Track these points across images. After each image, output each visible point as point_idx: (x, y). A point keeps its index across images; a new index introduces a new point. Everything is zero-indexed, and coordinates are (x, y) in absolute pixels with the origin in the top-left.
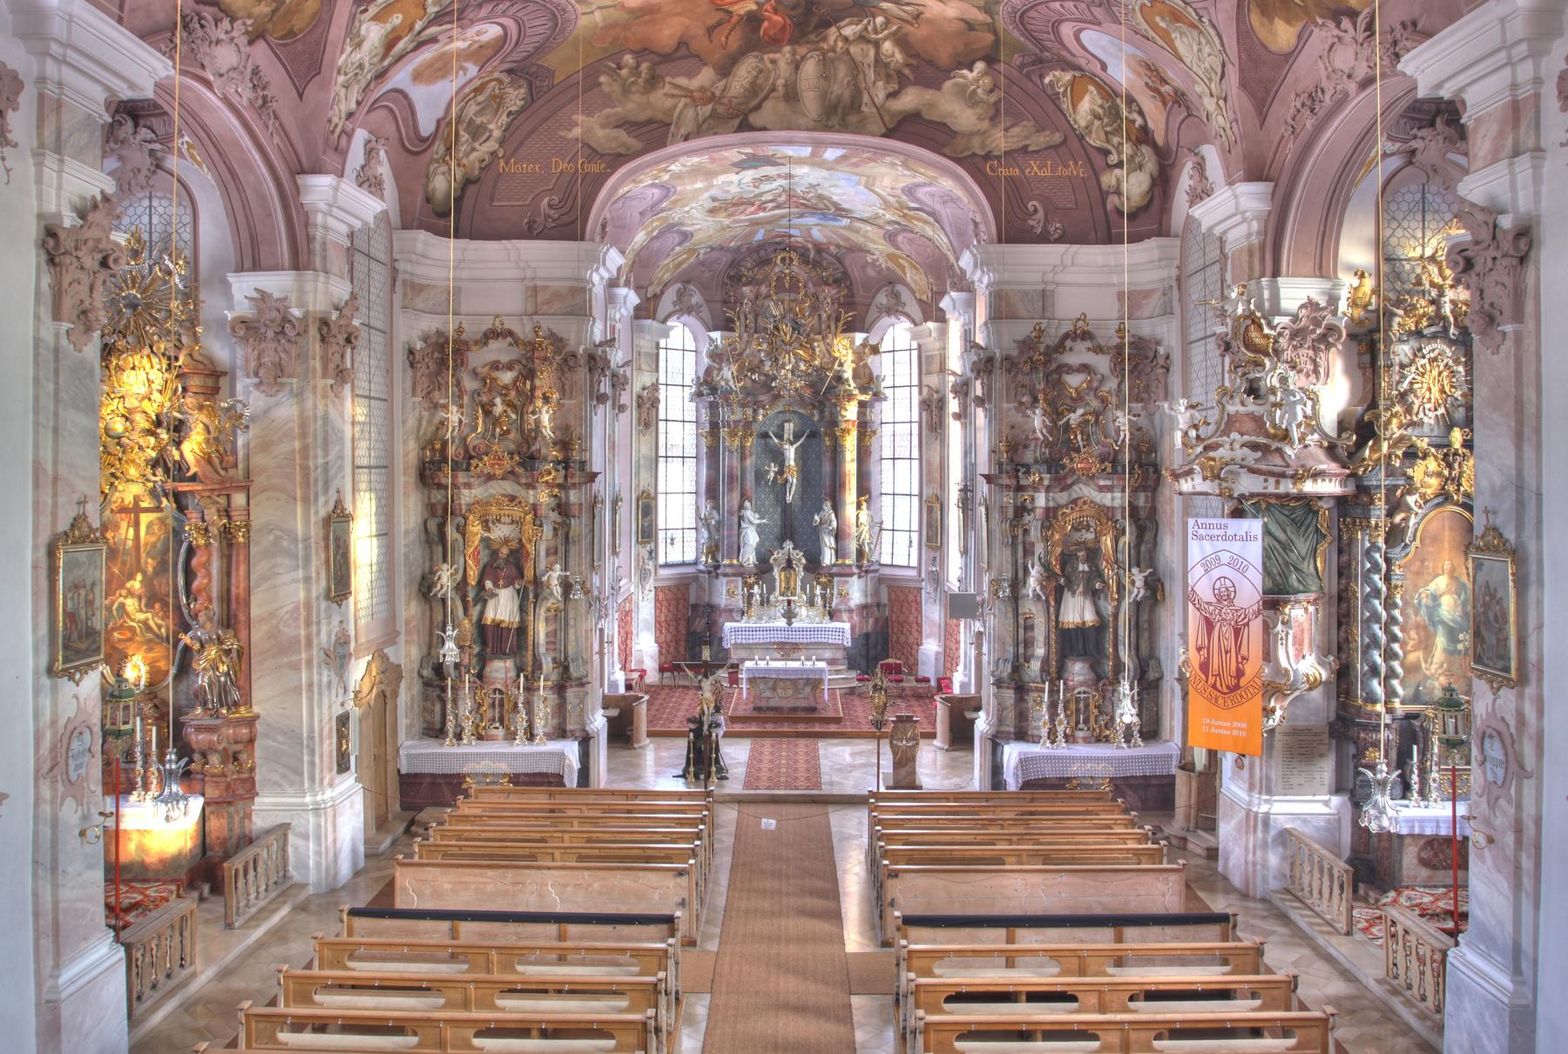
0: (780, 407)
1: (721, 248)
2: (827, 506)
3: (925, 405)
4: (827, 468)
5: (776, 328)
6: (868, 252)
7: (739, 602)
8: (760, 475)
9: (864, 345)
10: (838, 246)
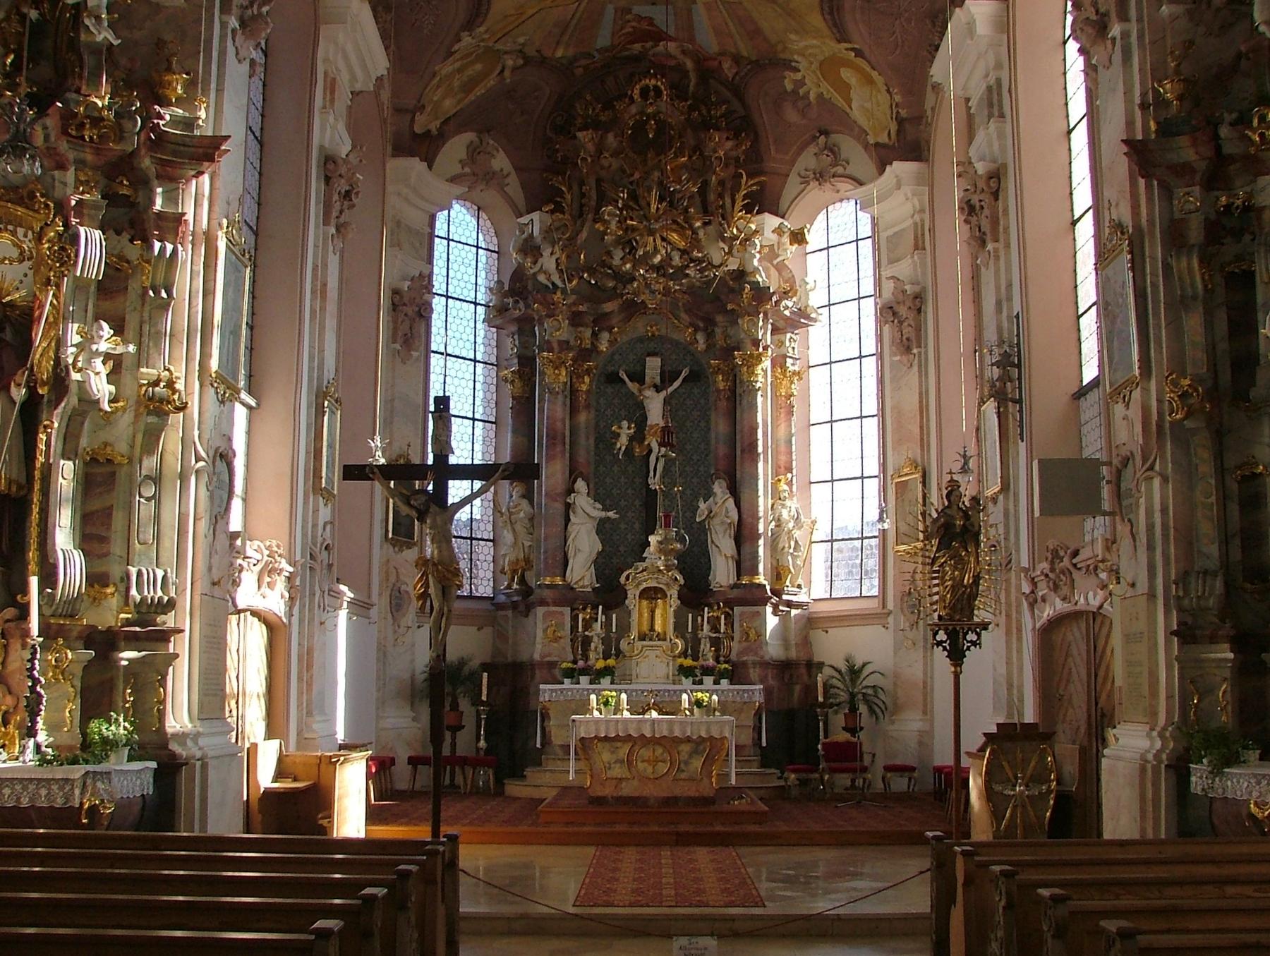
0: (640, 326)
1: (542, 62)
2: (719, 488)
3: (888, 313)
4: (720, 426)
5: (633, 196)
6: (789, 66)
7: (563, 653)
8: (605, 440)
9: (779, 231)
10: (737, 59)
